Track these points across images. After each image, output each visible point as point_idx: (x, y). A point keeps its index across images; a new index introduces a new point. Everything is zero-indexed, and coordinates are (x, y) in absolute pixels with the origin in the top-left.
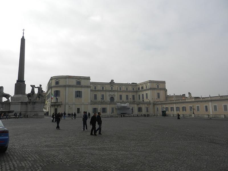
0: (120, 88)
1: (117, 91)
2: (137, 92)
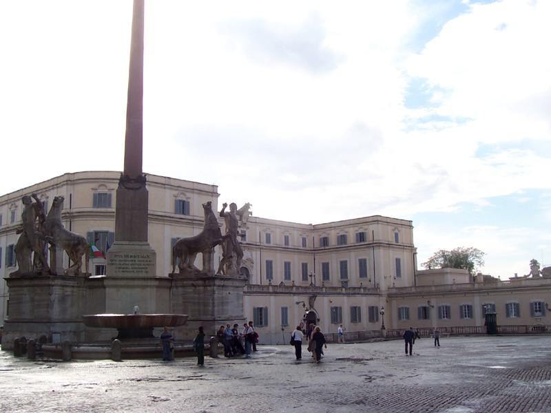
2: (314, 251)
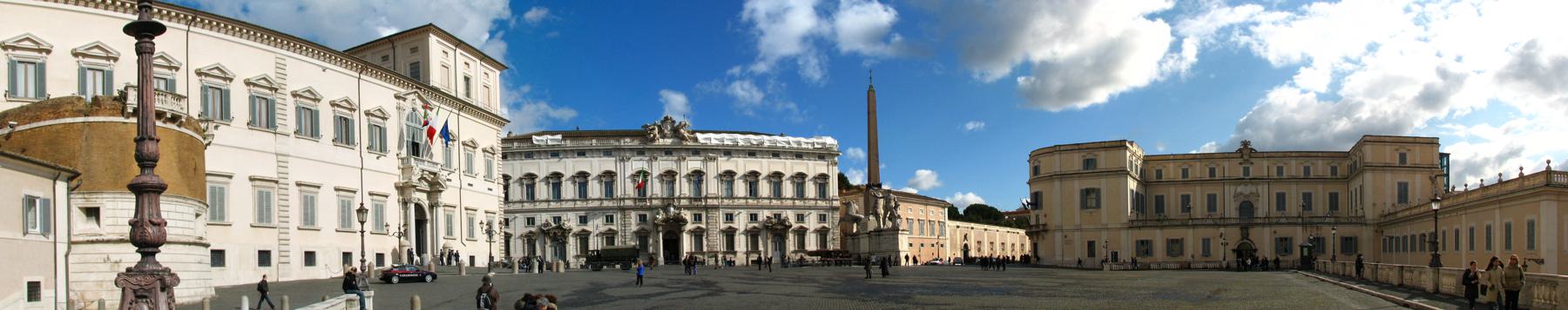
0: (1280, 170)
1: (1268, 180)
